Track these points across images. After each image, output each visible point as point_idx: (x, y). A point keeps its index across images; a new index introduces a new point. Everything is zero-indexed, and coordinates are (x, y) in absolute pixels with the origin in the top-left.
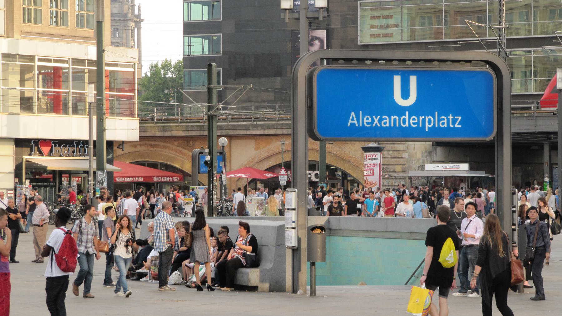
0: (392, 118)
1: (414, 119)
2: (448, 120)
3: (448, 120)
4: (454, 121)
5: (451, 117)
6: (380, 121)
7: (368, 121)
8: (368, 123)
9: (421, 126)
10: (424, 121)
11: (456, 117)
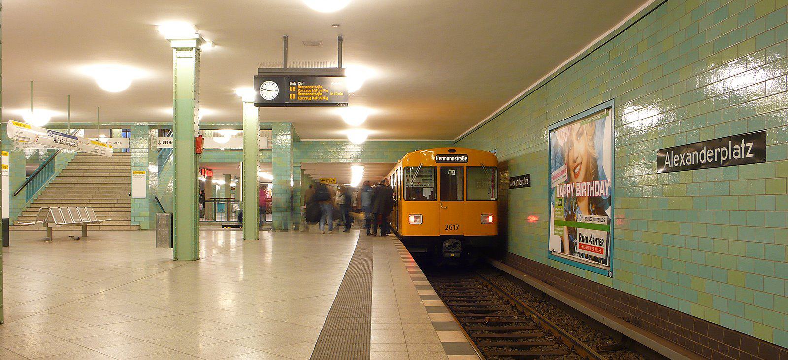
0: (694, 153)
1: (710, 153)
2: (741, 148)
3: (741, 148)
4: (746, 149)
5: (743, 145)
6: (684, 159)
7: (677, 160)
8: (676, 162)
9: (716, 161)
10: (719, 154)
11: (747, 145)
